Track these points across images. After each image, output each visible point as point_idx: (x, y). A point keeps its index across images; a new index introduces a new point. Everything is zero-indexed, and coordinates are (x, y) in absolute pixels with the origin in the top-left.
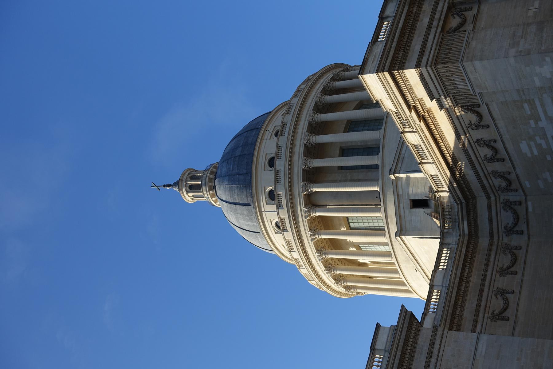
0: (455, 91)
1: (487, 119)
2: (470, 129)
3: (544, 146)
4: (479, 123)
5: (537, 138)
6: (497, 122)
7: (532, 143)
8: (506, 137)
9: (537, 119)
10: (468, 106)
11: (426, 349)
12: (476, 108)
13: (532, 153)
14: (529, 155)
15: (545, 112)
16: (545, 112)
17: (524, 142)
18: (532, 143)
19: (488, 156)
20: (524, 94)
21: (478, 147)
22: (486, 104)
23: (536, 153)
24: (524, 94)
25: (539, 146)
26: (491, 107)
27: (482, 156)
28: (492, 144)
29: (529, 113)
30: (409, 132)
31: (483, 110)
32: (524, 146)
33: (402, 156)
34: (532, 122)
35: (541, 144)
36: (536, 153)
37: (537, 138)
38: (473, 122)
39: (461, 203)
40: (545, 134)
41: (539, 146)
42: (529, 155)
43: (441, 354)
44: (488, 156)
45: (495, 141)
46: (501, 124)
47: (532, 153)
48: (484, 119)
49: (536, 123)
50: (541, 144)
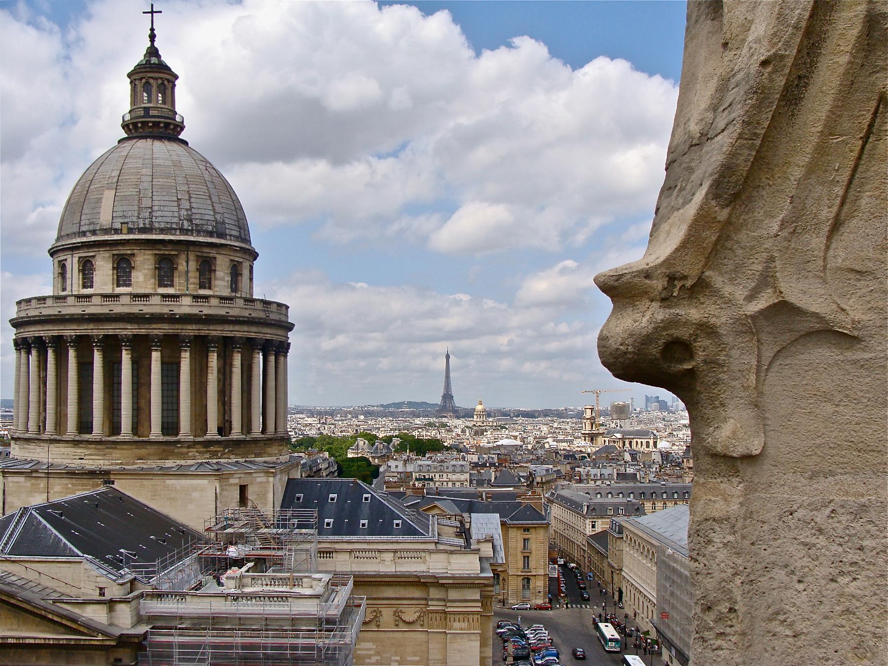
0: (452, 619)
2: (395, 609)
3: (367, 661)
5: (379, 658)
13: (359, 649)
18: (372, 652)
23: (359, 652)
25: (369, 656)
28: (374, 622)
29: (409, 658)
32: (369, 645)
34: (399, 658)
37: (379, 658)
41: (369, 656)
46: (399, 635)
47: (359, 649)
49: (396, 661)
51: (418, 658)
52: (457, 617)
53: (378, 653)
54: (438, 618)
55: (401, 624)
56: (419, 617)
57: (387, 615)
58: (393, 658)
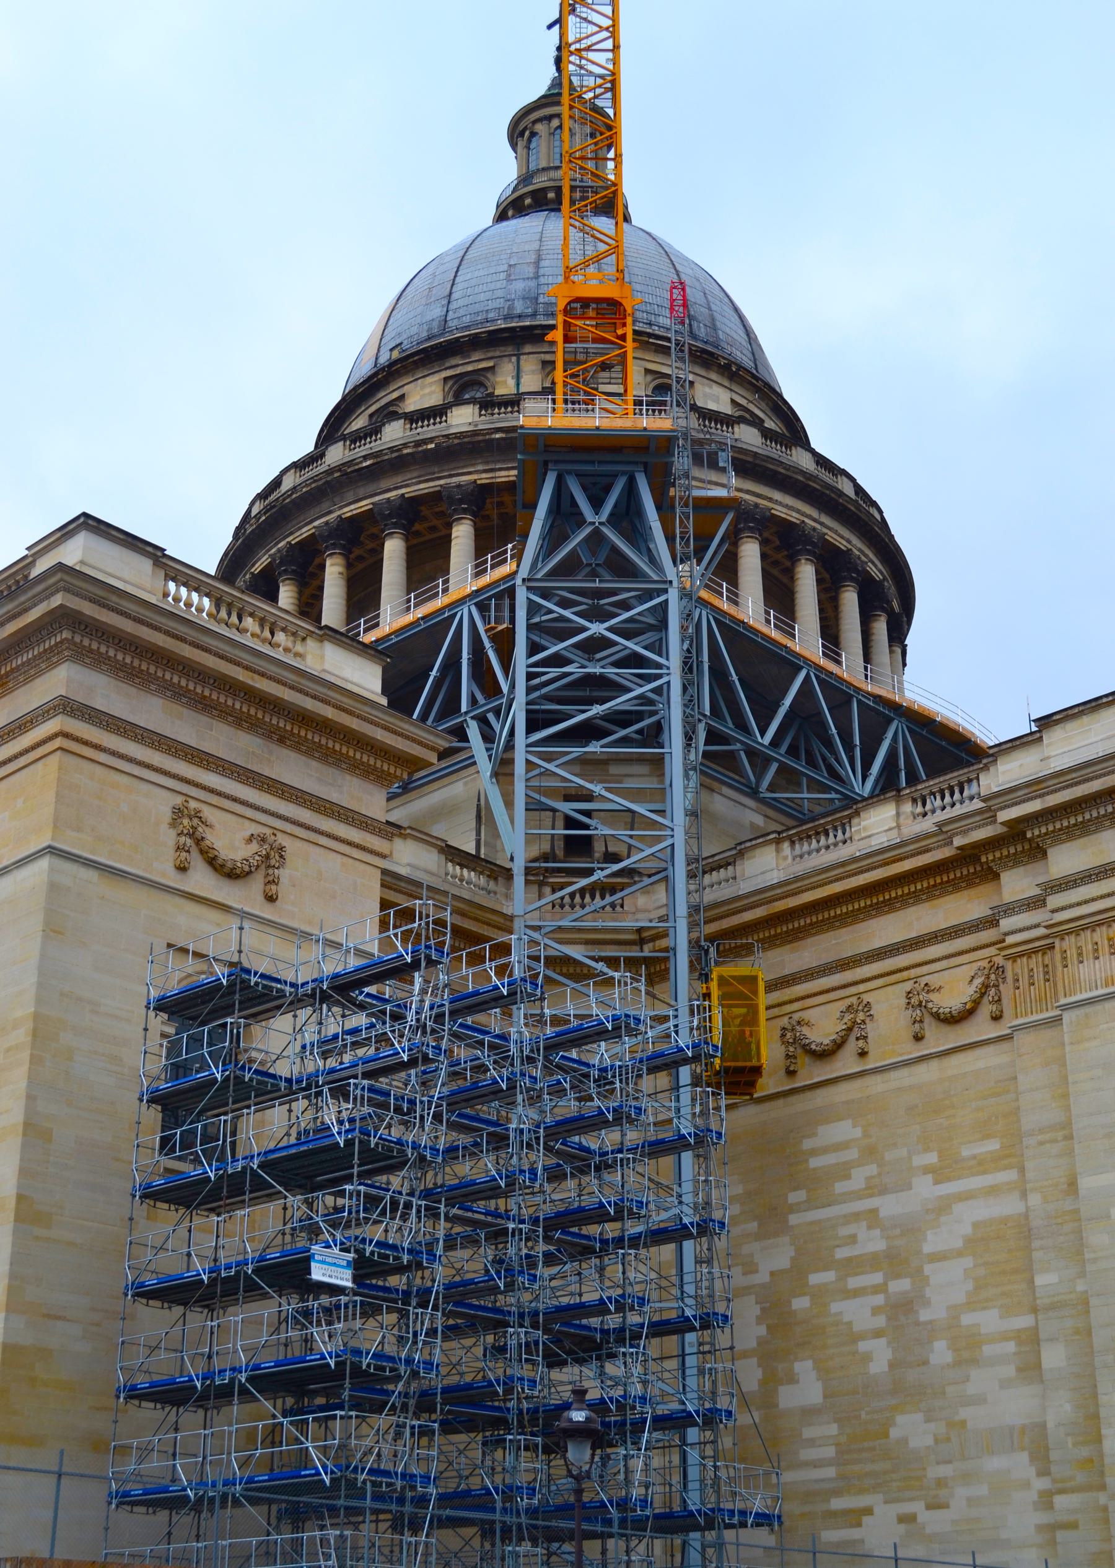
0: (1072, 953)
1: (938, 1038)
2: (908, 986)
3: (840, 1187)
4: (937, 1016)
5: (872, 1169)
6: (934, 1064)
7: (853, 1154)
8: (876, 1085)
9: (939, 1174)
10: (996, 986)
11: (334, 796)
12: (986, 1009)
13: (814, 1152)
14: (807, 1144)
15: (966, 1196)
16: (966, 1196)
17: (858, 1132)
18: (853, 1154)
19: (805, 1030)
20: (1041, 1143)
21: (842, 1005)
22: (1008, 1038)
23: (814, 1163)
24: (1041, 1143)
26: (990, 1049)
27: (806, 1015)
29: (966, 1152)
30: (898, 814)
31: (980, 1028)
33: (715, 785)
34: (932, 1158)
35: (848, 1177)
36: (814, 1163)
38: (933, 996)
39: (642, 942)
40: (883, 1191)
41: (843, 1172)
42: (807, 1144)
43: (323, 841)
44: (805, 1030)
45: (863, 1054)
47: (814, 1152)
48: (945, 1029)
49: (926, 1170)
50: (848, 1177)
51: (993, 1145)
52: (1086, 939)
53: (870, 1153)
54: (1039, 976)
55: (931, 1029)
56: (985, 988)
57: (888, 1009)
58: (919, 1161)
